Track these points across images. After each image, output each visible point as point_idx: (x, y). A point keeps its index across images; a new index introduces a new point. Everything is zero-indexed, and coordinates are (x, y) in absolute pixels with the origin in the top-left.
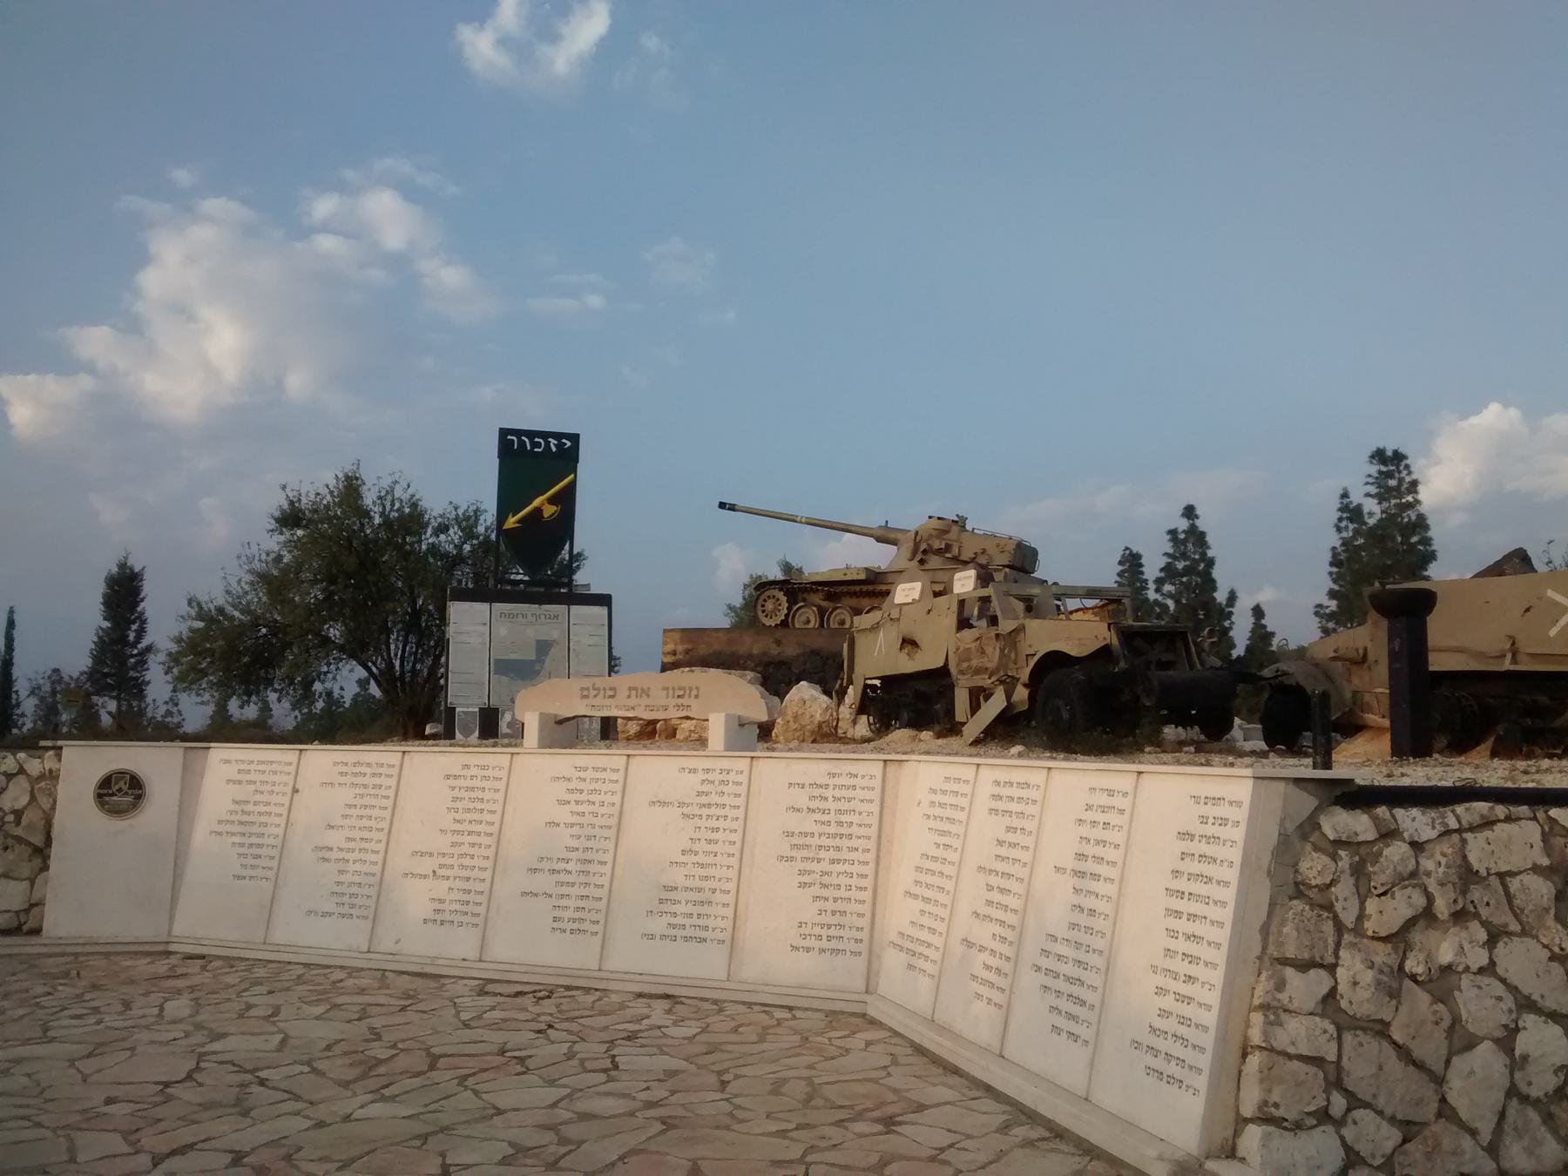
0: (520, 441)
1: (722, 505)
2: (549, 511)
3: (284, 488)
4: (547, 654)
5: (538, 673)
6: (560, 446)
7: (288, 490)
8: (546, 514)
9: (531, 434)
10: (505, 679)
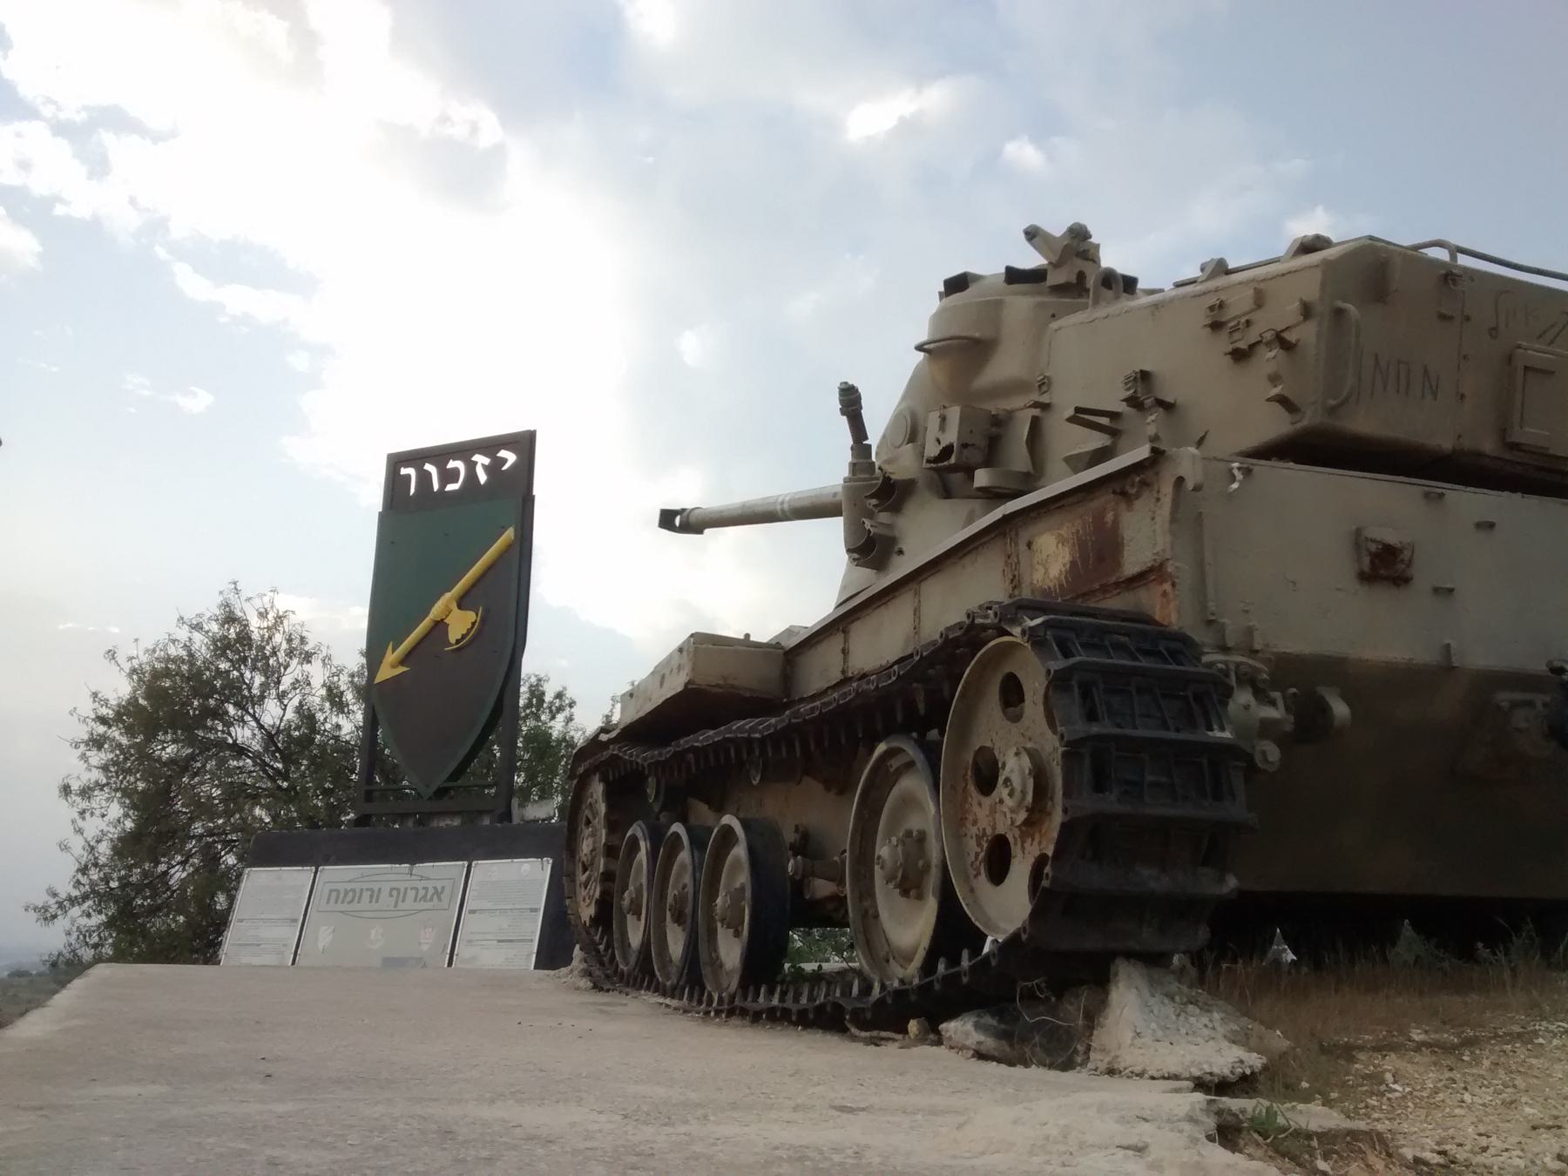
0: (424, 478)
1: (667, 519)
2: (460, 624)
3: (111, 655)
6: (495, 468)
7: (121, 658)
8: (454, 635)
9: (440, 455)
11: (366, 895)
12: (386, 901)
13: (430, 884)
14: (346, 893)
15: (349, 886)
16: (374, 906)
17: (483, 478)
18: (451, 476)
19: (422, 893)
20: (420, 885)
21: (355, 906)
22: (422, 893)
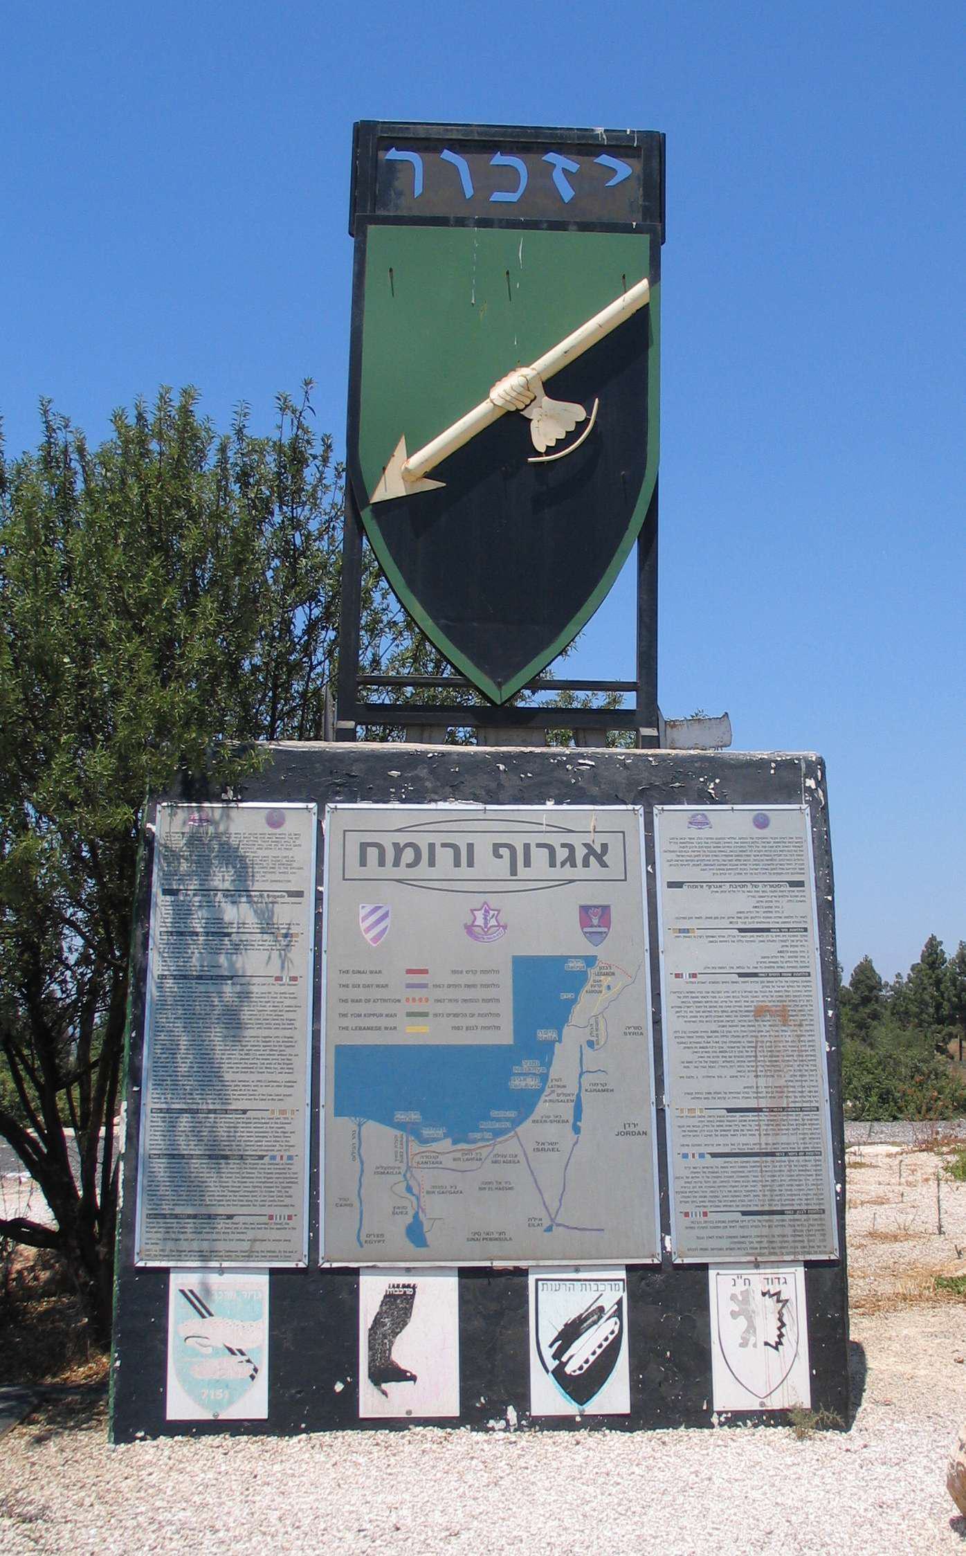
4: (559, 1018)
5: (525, 1104)
10: (379, 1138)
11: (444, 856)
12: (490, 866)
13: (577, 841)
14: (399, 849)
15: (402, 839)
16: (464, 872)
17: (567, 193)
18: (508, 178)
19: (562, 854)
20: (555, 840)
21: (423, 870)
22: (562, 854)
